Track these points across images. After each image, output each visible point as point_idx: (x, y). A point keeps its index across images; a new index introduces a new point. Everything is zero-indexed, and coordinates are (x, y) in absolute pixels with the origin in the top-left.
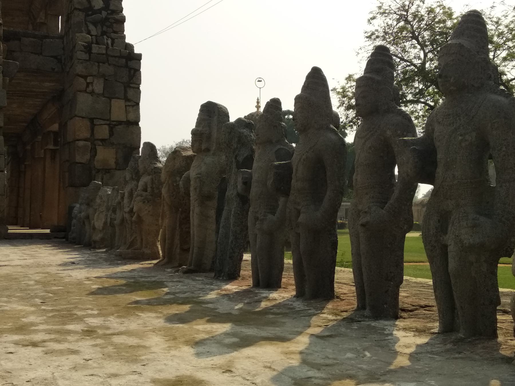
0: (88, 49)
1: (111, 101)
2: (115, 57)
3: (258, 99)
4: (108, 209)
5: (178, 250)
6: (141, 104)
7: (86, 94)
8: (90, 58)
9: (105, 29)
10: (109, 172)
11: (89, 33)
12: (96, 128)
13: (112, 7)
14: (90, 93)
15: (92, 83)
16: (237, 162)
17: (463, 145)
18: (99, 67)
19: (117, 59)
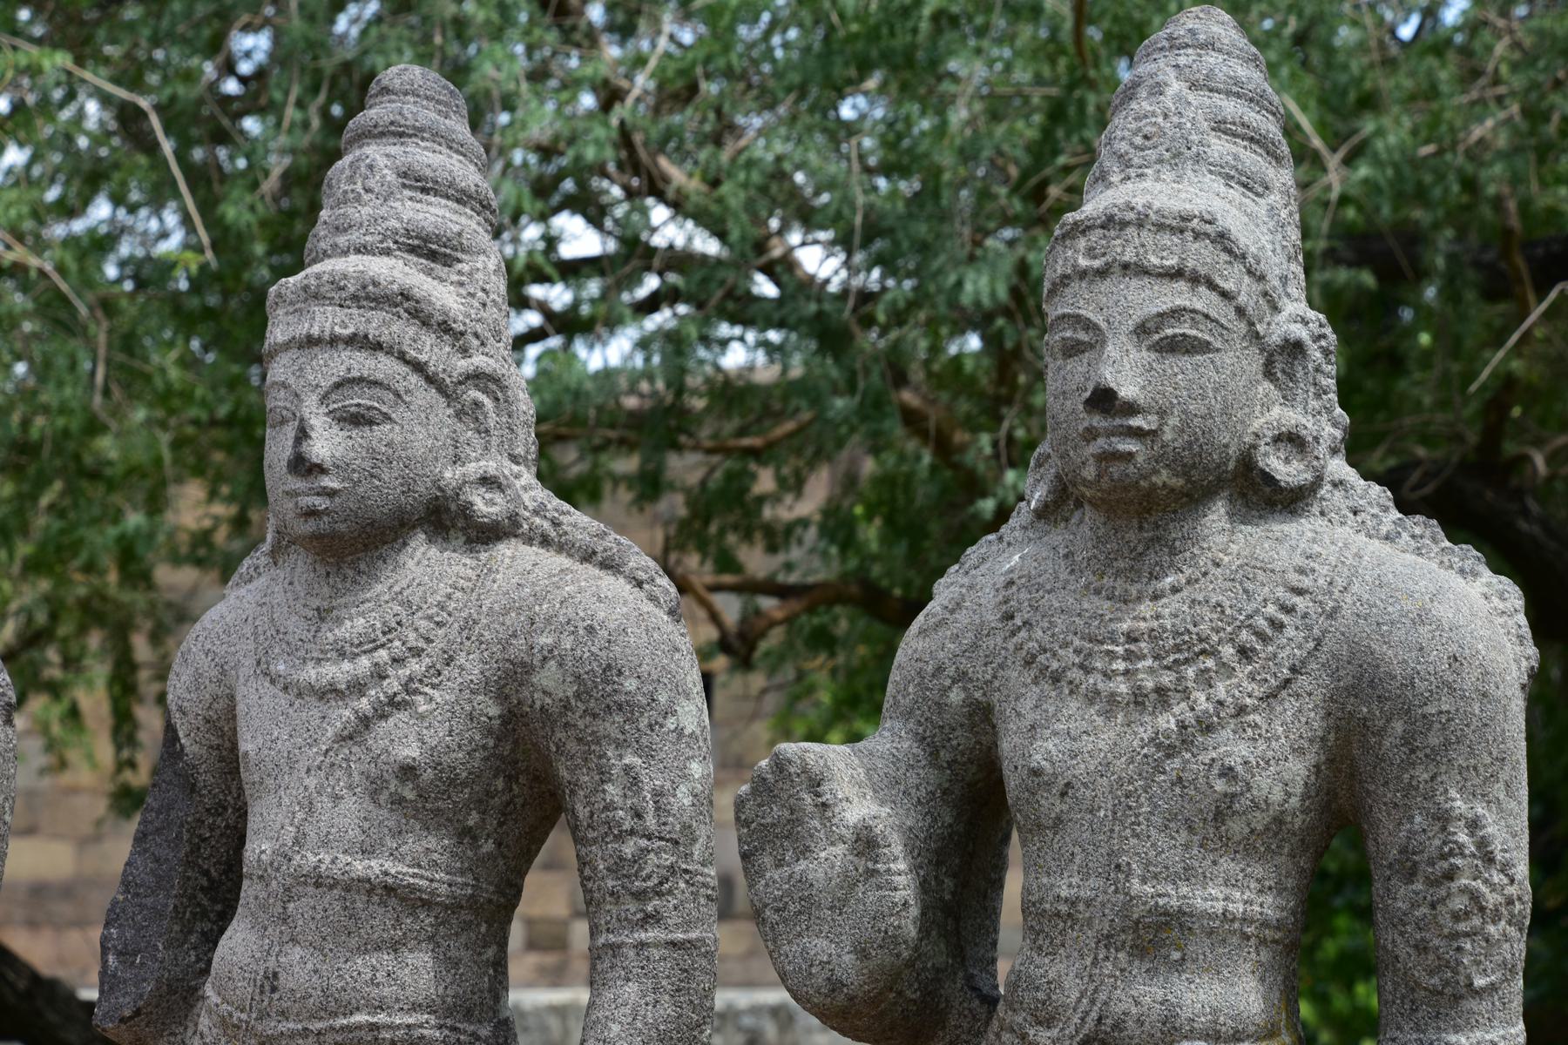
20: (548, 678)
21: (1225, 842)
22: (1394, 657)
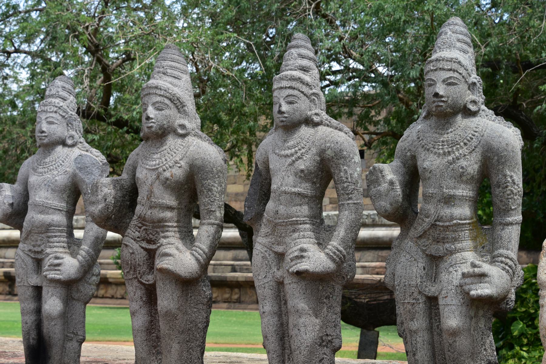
20: (329, 152)
21: (462, 181)
22: (495, 144)
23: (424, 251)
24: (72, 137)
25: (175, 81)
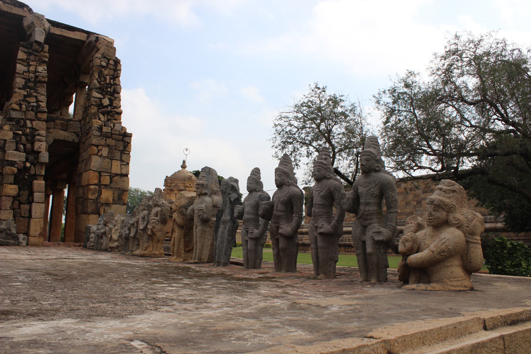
0: (100, 129)
1: (112, 161)
2: (116, 135)
3: (184, 162)
4: (122, 228)
5: (183, 252)
6: (130, 164)
7: (97, 157)
8: (101, 134)
9: (109, 117)
10: (108, 206)
11: (100, 119)
12: (102, 178)
13: (114, 105)
14: (100, 156)
15: (101, 150)
16: (231, 201)
17: (373, 196)
18: (106, 140)
19: (117, 136)
20: (332, 189)
23: (361, 224)
24: (258, 188)
25: (286, 167)
